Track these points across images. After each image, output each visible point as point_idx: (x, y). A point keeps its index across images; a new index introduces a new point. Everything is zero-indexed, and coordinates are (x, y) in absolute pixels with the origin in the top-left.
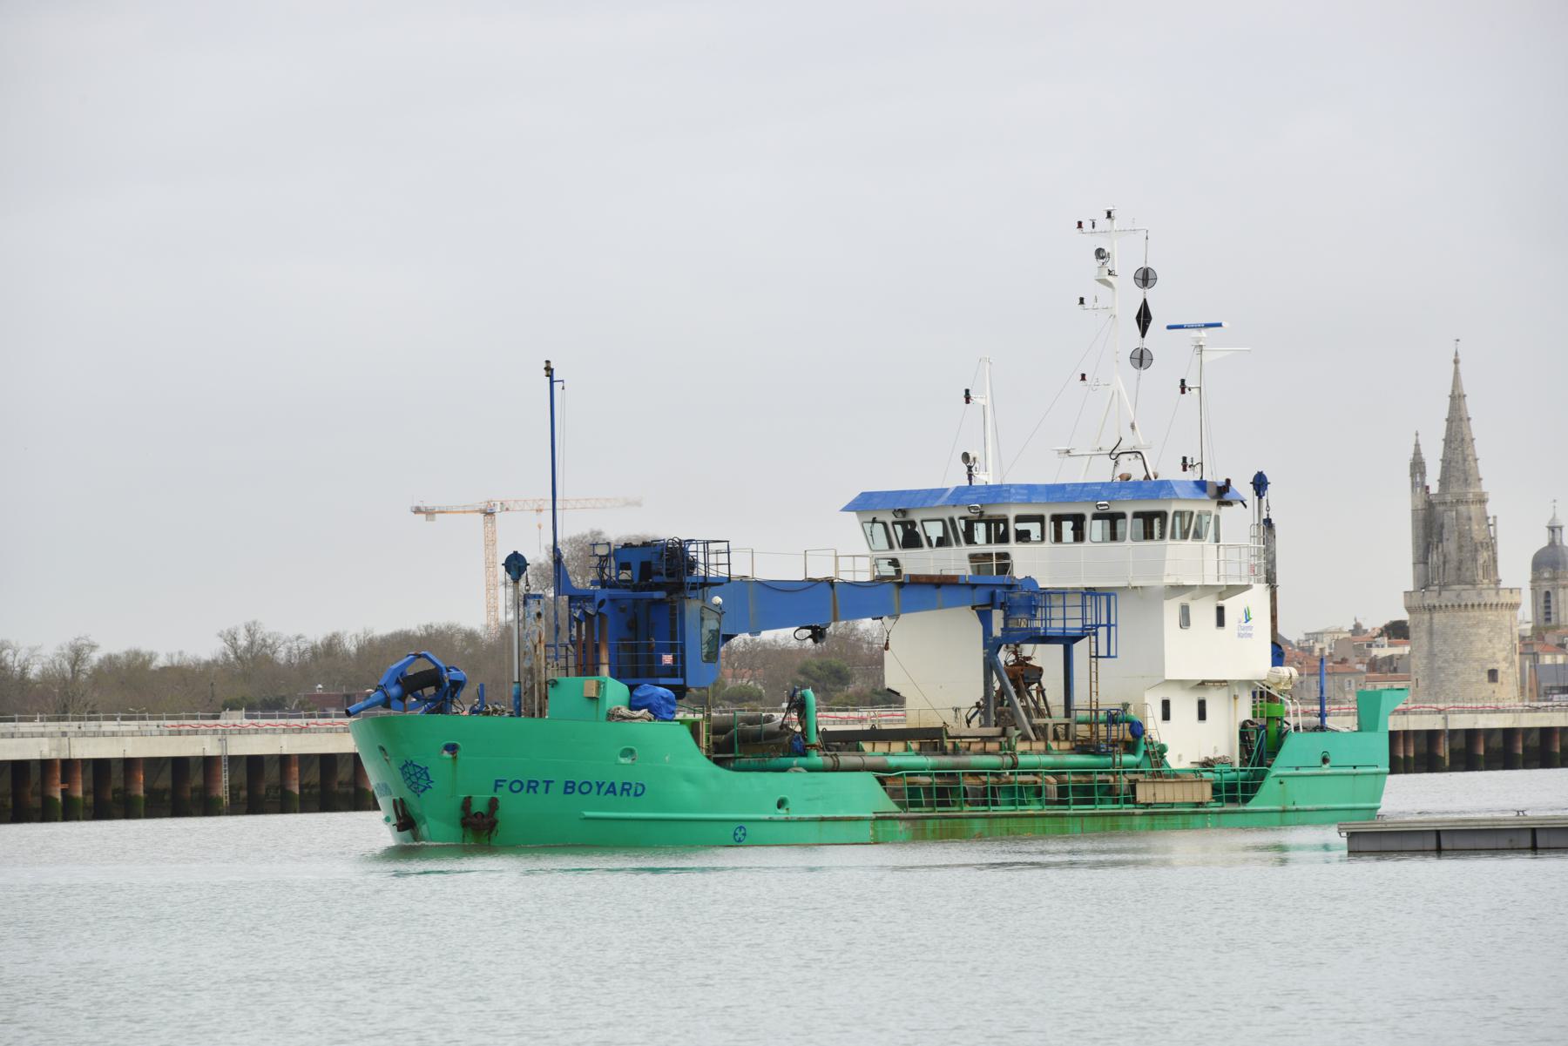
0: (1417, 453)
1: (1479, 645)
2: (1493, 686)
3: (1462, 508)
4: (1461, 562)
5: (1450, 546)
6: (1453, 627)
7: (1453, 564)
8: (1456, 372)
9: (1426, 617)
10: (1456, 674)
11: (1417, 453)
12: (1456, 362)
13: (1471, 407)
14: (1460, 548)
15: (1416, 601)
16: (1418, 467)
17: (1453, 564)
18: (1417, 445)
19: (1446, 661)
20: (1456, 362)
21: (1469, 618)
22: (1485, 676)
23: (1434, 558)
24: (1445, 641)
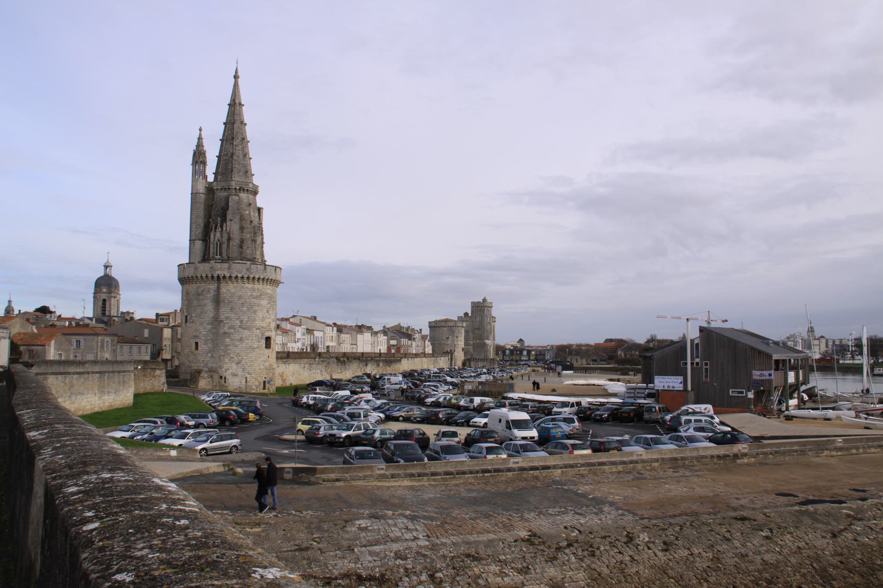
0: (200, 145)
2: (267, 351)
3: (243, 195)
4: (242, 241)
5: (233, 226)
6: (240, 297)
7: (235, 243)
8: (236, 86)
9: (213, 286)
10: (241, 340)
11: (200, 145)
12: (236, 77)
13: (248, 114)
14: (242, 229)
15: (190, 272)
16: (199, 157)
17: (235, 243)
18: (200, 139)
19: (231, 327)
20: (236, 77)
21: (254, 290)
22: (264, 342)
23: (215, 236)
24: (232, 309)
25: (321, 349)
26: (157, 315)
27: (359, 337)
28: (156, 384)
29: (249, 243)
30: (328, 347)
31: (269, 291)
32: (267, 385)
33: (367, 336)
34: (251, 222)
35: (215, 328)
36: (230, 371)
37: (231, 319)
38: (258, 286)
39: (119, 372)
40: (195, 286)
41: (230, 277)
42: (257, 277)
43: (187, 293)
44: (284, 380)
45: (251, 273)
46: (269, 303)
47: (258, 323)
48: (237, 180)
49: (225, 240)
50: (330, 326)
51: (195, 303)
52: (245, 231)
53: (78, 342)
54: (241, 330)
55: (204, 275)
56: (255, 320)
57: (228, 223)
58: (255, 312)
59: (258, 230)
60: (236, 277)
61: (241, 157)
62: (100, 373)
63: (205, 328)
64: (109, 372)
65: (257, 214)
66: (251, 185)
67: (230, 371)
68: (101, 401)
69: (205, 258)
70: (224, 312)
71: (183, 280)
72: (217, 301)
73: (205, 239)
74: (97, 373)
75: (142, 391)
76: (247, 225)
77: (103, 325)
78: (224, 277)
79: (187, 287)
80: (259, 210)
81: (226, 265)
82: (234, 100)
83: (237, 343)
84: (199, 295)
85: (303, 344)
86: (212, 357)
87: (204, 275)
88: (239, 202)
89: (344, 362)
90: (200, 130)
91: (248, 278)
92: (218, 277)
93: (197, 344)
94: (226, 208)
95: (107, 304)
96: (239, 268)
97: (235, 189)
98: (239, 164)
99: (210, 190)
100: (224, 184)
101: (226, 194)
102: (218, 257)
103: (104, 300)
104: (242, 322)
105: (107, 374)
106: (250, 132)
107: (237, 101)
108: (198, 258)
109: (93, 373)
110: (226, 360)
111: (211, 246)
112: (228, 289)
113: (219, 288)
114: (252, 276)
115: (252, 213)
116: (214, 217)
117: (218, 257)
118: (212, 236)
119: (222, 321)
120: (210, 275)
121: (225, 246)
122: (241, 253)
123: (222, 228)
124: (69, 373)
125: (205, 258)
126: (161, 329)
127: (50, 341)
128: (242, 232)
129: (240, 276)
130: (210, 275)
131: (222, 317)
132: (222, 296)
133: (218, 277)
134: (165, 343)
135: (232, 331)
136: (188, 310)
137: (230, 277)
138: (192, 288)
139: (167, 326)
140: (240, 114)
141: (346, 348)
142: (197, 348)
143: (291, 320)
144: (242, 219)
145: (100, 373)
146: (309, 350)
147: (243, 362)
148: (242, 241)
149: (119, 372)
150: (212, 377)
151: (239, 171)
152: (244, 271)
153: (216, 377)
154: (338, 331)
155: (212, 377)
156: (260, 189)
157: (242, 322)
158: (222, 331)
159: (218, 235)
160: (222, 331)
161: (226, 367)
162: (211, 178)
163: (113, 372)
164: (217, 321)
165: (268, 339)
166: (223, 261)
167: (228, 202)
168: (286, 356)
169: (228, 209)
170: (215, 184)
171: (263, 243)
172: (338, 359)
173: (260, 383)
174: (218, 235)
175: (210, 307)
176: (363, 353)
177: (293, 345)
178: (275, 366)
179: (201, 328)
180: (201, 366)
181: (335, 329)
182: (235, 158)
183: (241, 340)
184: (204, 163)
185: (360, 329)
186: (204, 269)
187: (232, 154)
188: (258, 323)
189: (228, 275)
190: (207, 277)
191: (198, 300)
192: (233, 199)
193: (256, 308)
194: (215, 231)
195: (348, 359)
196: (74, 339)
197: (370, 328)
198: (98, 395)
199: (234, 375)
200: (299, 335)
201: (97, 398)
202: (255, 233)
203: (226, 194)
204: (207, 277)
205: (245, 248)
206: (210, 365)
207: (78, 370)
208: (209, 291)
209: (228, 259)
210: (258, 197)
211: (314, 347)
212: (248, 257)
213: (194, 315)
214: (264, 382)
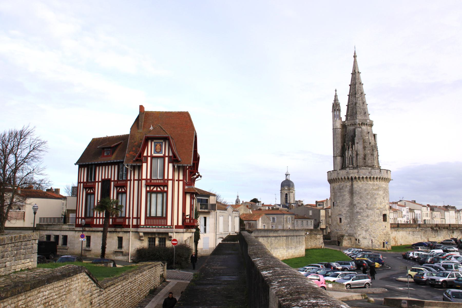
0: (336, 100)
1: (379, 200)
3: (364, 127)
4: (365, 155)
5: (359, 147)
6: (366, 190)
7: (361, 156)
8: (355, 62)
9: (349, 184)
10: (367, 216)
11: (336, 100)
12: (355, 57)
13: (363, 78)
14: (364, 148)
15: (334, 176)
16: (336, 107)
17: (361, 156)
18: (336, 96)
19: (361, 208)
20: (355, 57)
21: (374, 185)
22: (382, 217)
23: (348, 153)
24: (361, 198)
25: (420, 222)
26: (317, 202)
27: (446, 213)
28: (318, 243)
29: (369, 156)
30: (425, 220)
31: (384, 186)
32: (385, 245)
33: (452, 213)
34: (370, 143)
35: (351, 209)
36: (362, 236)
37: (361, 204)
38: (376, 182)
39: (297, 236)
40: (338, 184)
41: (359, 178)
42: (376, 177)
43: (334, 189)
44: (396, 242)
45: (372, 175)
46: (384, 193)
47: (378, 206)
48: (359, 118)
49: (354, 155)
50: (425, 206)
51: (339, 194)
52: (367, 149)
53: (273, 218)
54: (367, 210)
55: (343, 177)
56: (375, 204)
57: (356, 145)
58: (375, 199)
59: (374, 148)
60: (363, 178)
61: (361, 104)
62: (286, 236)
63: (345, 209)
64: (291, 236)
65: (373, 138)
66: (368, 121)
67: (362, 236)
68: (288, 253)
69: (343, 167)
70: (356, 199)
71: (331, 181)
72: (352, 192)
73: (343, 155)
74: (284, 236)
75: (309, 247)
76: (367, 145)
77: (286, 209)
78: (355, 178)
79: (333, 185)
80: (375, 135)
81: (356, 171)
82: (355, 71)
83: (365, 218)
84: (340, 189)
85: (408, 219)
86: (350, 227)
87: (343, 177)
88: (361, 132)
89: (436, 231)
90: (336, 91)
91: (370, 178)
92: (352, 178)
93: (340, 219)
94: (354, 136)
95: (288, 196)
96: (364, 172)
97: (359, 124)
98: (360, 109)
99: (344, 126)
100: (352, 122)
101: (353, 127)
102: (351, 166)
103: (286, 194)
104: (367, 205)
105: (290, 237)
106: (366, 88)
107: (356, 71)
108: (339, 167)
109: (282, 236)
110: (359, 229)
111: (347, 159)
112: (358, 185)
113: (352, 185)
114: (372, 177)
115: (370, 138)
116: (347, 142)
117: (351, 166)
118: (347, 154)
119: (355, 205)
120: (346, 177)
121: (354, 159)
122: (365, 163)
123: (352, 148)
124: (270, 237)
125: (343, 167)
126: (319, 210)
127: (259, 218)
128: (365, 150)
129: (365, 177)
130: (346, 177)
131: (355, 202)
132: (355, 189)
133: (352, 178)
134: (321, 219)
135: (362, 211)
136: (334, 198)
137: (359, 178)
138: (336, 185)
139: (323, 209)
140: (359, 78)
141: (438, 221)
142: (341, 222)
143: (399, 203)
144: (364, 142)
145: (286, 236)
146: (412, 222)
147: (369, 230)
148: (365, 155)
149: (297, 236)
150: (350, 239)
151: (361, 113)
152: (368, 173)
153: (353, 239)
154: (431, 210)
155: (350, 239)
156: (374, 123)
157: (367, 205)
158: (355, 211)
159: (350, 152)
160: (355, 211)
161: (359, 233)
162: (344, 119)
163: (293, 236)
164: (352, 205)
165: (385, 216)
166: (354, 168)
167: (355, 132)
168: (397, 226)
169: (355, 136)
170: (346, 122)
171: (378, 156)
172: (432, 228)
173: (381, 243)
174: (350, 152)
175: (347, 196)
176: (450, 225)
177: (401, 219)
178: (390, 232)
179: (343, 210)
180: (344, 232)
181: (429, 208)
182: (357, 105)
183: (367, 216)
184: (339, 110)
185: (447, 208)
186: (343, 173)
187: (356, 103)
188: (378, 206)
189: (357, 177)
190: (345, 178)
191: (340, 192)
192: (358, 130)
193: (376, 196)
194: (348, 150)
195: (439, 228)
196: (271, 217)
197: (453, 208)
198: (286, 249)
199: (365, 238)
200: (404, 213)
201: (285, 251)
202: (373, 150)
203: (353, 127)
204: (345, 178)
205: (367, 159)
206: (349, 232)
207: (275, 235)
208: (346, 186)
209: (357, 167)
210: (373, 127)
211: (415, 220)
212: (370, 165)
213: (338, 201)
214: (384, 243)
